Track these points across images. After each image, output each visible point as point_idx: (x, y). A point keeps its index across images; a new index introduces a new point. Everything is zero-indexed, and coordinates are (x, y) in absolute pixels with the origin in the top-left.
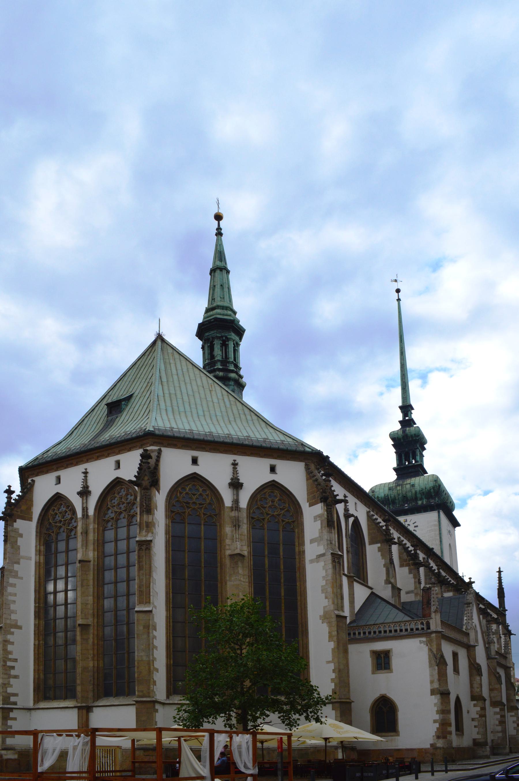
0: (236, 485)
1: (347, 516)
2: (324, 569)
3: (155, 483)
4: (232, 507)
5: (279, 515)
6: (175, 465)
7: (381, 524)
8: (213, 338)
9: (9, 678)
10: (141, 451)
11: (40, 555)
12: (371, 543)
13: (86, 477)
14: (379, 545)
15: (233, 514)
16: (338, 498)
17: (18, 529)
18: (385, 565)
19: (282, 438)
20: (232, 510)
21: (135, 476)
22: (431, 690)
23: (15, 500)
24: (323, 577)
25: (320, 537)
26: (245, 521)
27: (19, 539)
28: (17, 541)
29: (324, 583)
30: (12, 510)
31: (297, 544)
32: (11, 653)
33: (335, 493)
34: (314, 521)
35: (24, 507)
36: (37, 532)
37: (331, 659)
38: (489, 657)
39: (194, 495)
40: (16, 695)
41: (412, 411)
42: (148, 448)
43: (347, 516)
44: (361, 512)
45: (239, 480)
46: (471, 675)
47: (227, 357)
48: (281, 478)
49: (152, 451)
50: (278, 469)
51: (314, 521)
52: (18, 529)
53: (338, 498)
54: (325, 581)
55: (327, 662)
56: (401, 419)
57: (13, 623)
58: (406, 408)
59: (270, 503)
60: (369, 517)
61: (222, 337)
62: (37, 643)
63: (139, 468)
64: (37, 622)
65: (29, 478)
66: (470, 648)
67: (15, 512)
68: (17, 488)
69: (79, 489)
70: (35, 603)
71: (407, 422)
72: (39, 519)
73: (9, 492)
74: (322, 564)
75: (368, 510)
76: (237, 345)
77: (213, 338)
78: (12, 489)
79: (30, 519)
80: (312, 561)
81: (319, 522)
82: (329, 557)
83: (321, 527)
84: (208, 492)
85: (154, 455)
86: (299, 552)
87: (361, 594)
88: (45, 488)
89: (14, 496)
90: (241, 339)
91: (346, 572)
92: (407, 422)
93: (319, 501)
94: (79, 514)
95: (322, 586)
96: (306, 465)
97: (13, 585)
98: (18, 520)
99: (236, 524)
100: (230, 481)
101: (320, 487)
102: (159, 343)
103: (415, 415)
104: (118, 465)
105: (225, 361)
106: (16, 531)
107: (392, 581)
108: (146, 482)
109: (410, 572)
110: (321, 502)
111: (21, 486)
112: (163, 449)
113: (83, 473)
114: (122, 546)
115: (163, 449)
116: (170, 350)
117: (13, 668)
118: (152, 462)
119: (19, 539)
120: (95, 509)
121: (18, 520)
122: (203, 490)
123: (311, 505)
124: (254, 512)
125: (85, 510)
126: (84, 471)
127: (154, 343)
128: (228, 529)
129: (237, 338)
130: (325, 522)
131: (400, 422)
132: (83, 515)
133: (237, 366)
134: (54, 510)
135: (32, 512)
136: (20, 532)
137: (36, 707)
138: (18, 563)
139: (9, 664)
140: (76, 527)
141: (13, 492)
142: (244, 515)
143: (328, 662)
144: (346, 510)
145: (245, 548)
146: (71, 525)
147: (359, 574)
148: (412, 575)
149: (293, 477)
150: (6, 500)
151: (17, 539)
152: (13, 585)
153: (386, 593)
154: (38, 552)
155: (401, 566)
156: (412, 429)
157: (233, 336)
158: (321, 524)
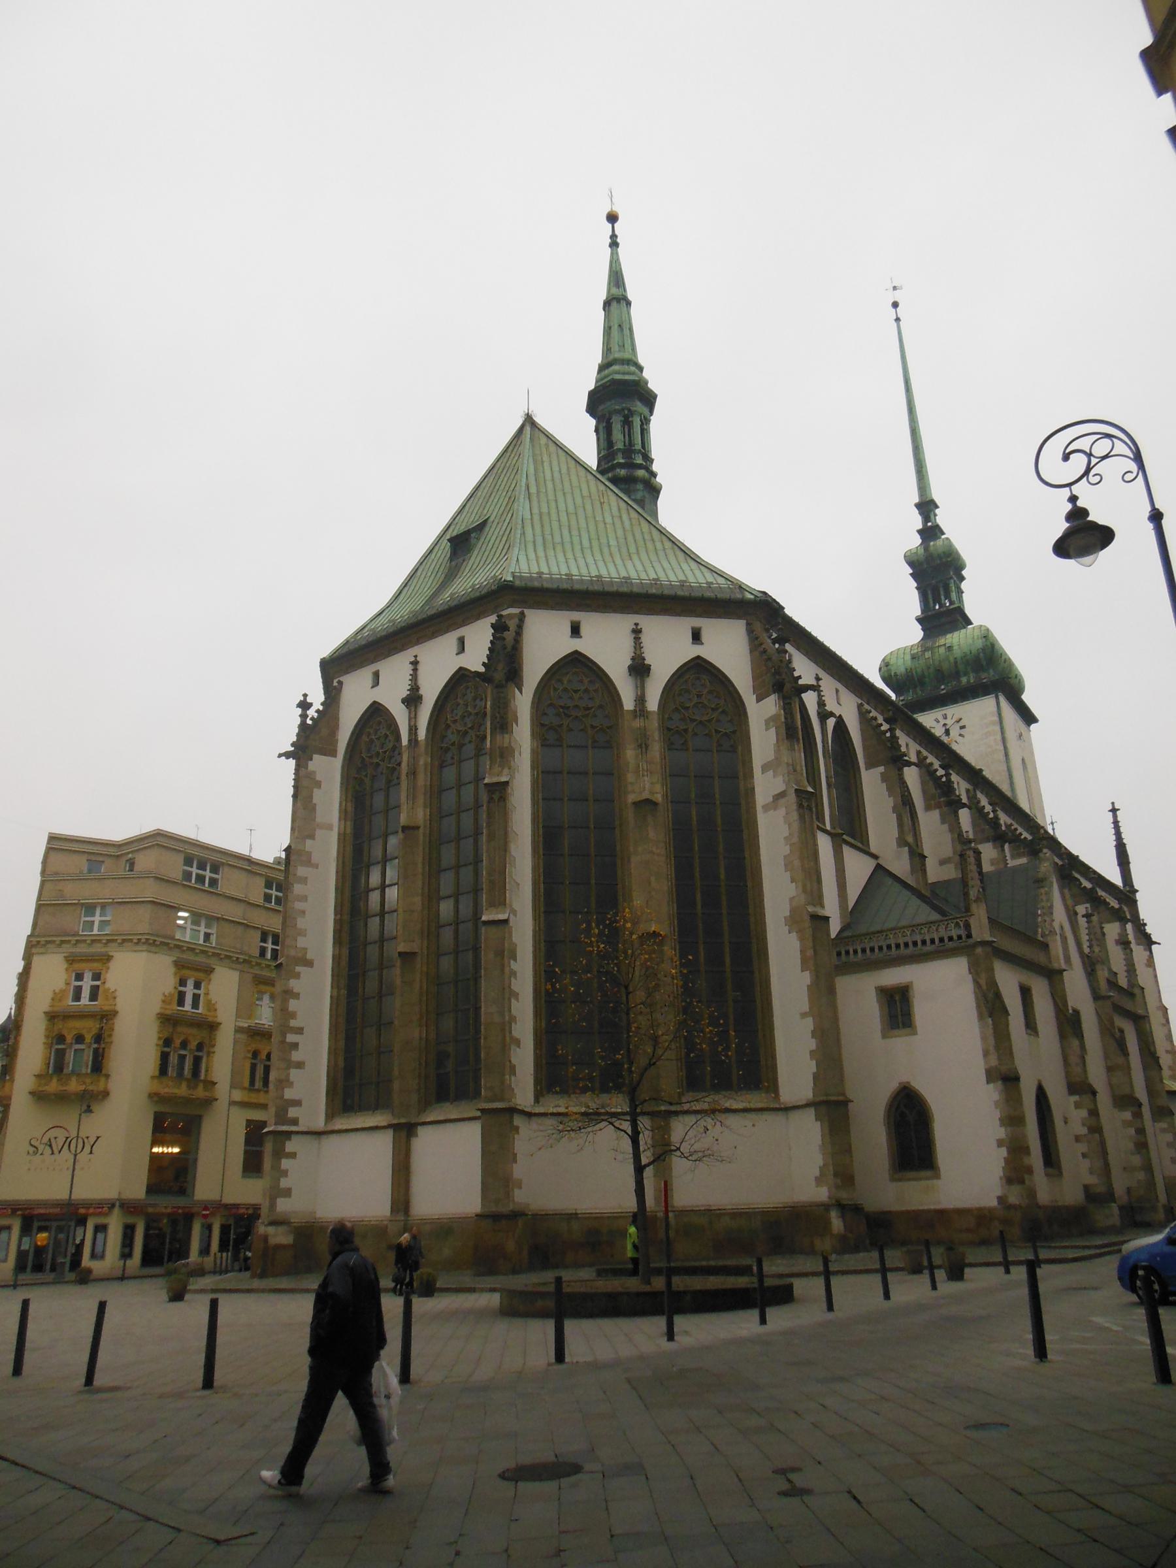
0: (639, 669)
1: (824, 715)
3: (514, 675)
4: (635, 711)
5: (709, 721)
6: (546, 640)
7: (883, 728)
8: (611, 413)
9: (288, 1068)
10: (493, 619)
11: (345, 820)
12: (870, 766)
13: (415, 670)
14: (882, 769)
15: (638, 723)
16: (801, 682)
17: (314, 772)
18: (895, 809)
19: (710, 578)
20: (636, 717)
21: (484, 664)
23: (312, 719)
25: (776, 758)
26: (656, 735)
27: (315, 790)
28: (311, 797)
31: (741, 775)
32: (293, 1015)
33: (796, 674)
38: (1097, 997)
39: (576, 691)
40: (297, 1103)
41: (937, 511)
42: (504, 613)
43: (824, 715)
44: (847, 707)
45: (644, 659)
46: (1062, 1036)
47: (631, 444)
49: (510, 616)
50: (705, 636)
53: (801, 682)
56: (920, 526)
57: (300, 955)
58: (927, 507)
59: (695, 700)
60: (863, 715)
61: (623, 409)
62: (335, 994)
63: (490, 649)
66: (1053, 976)
68: (317, 698)
71: (930, 532)
73: (304, 705)
75: (860, 701)
76: (645, 422)
77: (611, 413)
78: (309, 700)
79: (332, 753)
81: (773, 730)
84: (597, 685)
85: (512, 624)
87: (858, 869)
88: (357, 695)
89: (312, 713)
90: (651, 412)
91: (828, 827)
92: (930, 532)
96: (748, 624)
97: (304, 880)
98: (315, 756)
100: (629, 662)
101: (770, 664)
102: (528, 429)
103: (942, 518)
104: (461, 648)
105: (629, 451)
106: (311, 776)
107: (910, 839)
108: (499, 676)
109: (943, 821)
111: (325, 694)
112: (526, 611)
113: (411, 663)
114: (468, 793)
115: (526, 611)
116: (543, 440)
117: (295, 1046)
118: (509, 636)
119: (315, 790)
120: (428, 729)
121: (315, 756)
122: (590, 682)
123: (759, 699)
124: (670, 719)
125: (413, 730)
126: (413, 659)
127: (521, 430)
129: (645, 410)
131: (919, 532)
133: (648, 459)
134: (369, 734)
135: (337, 741)
136: (318, 778)
137: (330, 1128)
138: (312, 837)
139: (291, 1038)
141: (310, 705)
142: (654, 724)
144: (821, 704)
146: (393, 760)
147: (851, 830)
148: (946, 827)
150: (298, 721)
152: (304, 880)
153: (900, 865)
154: (344, 814)
155: (928, 808)
156: (939, 543)
157: (639, 407)
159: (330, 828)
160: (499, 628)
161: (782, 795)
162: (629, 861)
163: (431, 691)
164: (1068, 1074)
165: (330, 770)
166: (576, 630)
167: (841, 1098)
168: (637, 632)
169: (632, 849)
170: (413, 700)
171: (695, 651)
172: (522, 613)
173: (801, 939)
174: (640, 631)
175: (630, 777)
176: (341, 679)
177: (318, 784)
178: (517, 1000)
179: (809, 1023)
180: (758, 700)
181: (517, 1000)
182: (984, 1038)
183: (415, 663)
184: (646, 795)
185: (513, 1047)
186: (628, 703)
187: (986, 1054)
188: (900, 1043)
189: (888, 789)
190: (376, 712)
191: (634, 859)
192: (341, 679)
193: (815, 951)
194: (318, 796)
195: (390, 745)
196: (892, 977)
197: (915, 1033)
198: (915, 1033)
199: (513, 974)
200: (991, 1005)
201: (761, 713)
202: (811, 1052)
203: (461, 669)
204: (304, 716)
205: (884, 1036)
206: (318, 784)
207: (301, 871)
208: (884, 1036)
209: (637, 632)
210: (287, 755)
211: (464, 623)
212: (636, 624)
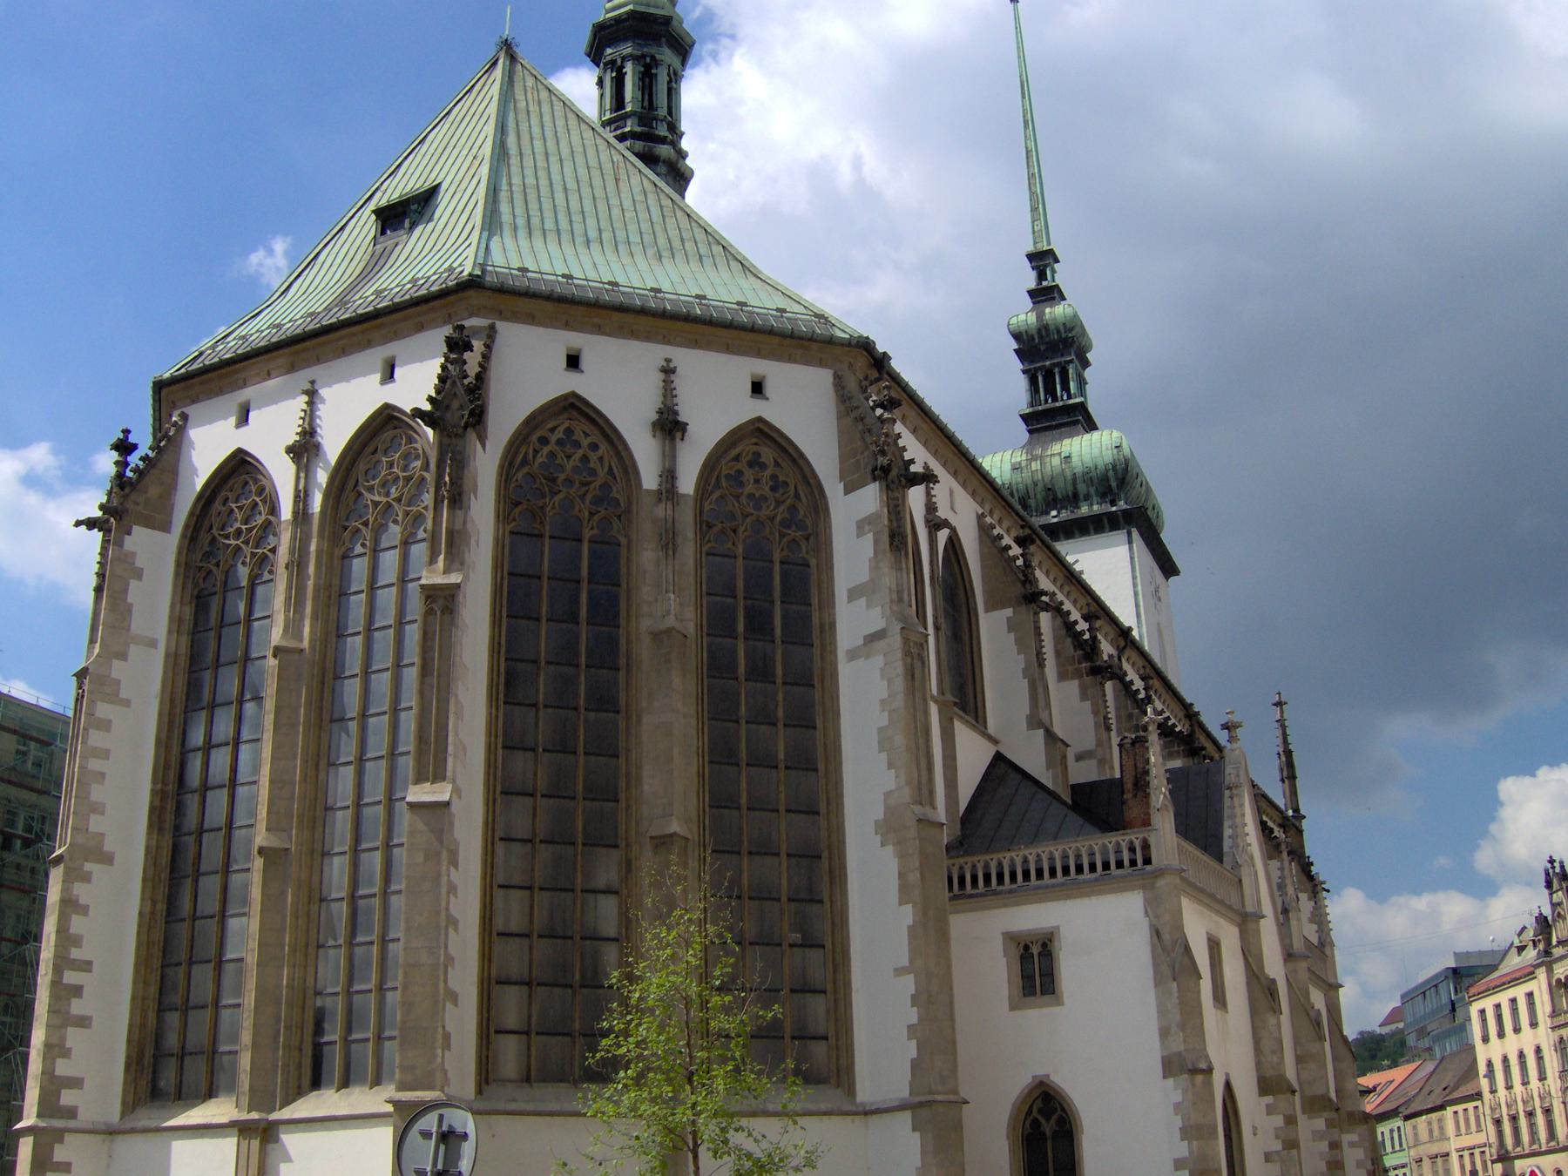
2: (882, 677)
15: (661, 511)
16: (913, 469)
17: (133, 554)
22: (1163, 1058)
23: (136, 470)
24: (882, 701)
25: (872, 580)
26: (690, 535)
27: (133, 583)
28: (126, 591)
29: (884, 720)
30: (126, 497)
31: (815, 601)
33: (907, 456)
34: (858, 536)
35: (154, 491)
36: (178, 564)
37: (905, 962)
48: (773, 411)
51: (858, 536)
52: (133, 554)
53: (913, 469)
54: (886, 714)
55: (896, 970)
64: (154, 843)
65: (174, 406)
67: (130, 505)
68: (144, 440)
69: (292, 438)
70: (154, 781)
72: (187, 526)
74: (878, 661)
78: (132, 439)
79: (165, 527)
80: (853, 655)
82: (895, 640)
83: (876, 552)
86: (822, 625)
89: (134, 459)
93: (870, 476)
94: (286, 512)
95: (880, 730)
97: (105, 725)
98: (136, 529)
99: (669, 542)
101: (869, 440)
106: (127, 559)
110: (874, 479)
119: (133, 583)
121: (136, 529)
125: (302, 498)
126: (307, 386)
128: (647, 556)
130: (885, 538)
132: (295, 513)
134: (226, 500)
135: (172, 507)
136: (138, 564)
138: (123, 656)
140: (273, 551)
141: (134, 447)
143: (900, 971)
145: (690, 612)
149: (804, 408)
151: (127, 585)
152: (105, 725)
154: (176, 621)
158: (876, 542)
159: (153, 644)
160: (457, 346)
161: (879, 635)
162: (639, 721)
163: (334, 441)
164: (1258, 1064)
165: (157, 552)
166: (573, 362)
167: (952, 1098)
168: (668, 371)
169: (644, 704)
170: (304, 449)
171: (751, 409)
172: (492, 327)
173: (902, 856)
174: (673, 371)
175: (646, 592)
176: (186, 410)
177: (138, 574)
178: (456, 930)
179: (908, 984)
180: (847, 491)
181: (456, 930)
182: (1162, 1012)
183: (312, 394)
184: (670, 622)
185: (448, 1005)
186: (650, 479)
187: (1164, 1033)
188: (1037, 1016)
189: (1018, 642)
190: (240, 466)
191: (647, 719)
192: (186, 410)
193: (922, 874)
194: (136, 592)
195: (260, 520)
196: (1031, 917)
197: (1059, 1002)
198: (1059, 1002)
199: (452, 888)
200: (1173, 961)
201: (852, 511)
202: (909, 1027)
203: (387, 406)
204: (122, 465)
205: (1013, 1007)
206: (138, 574)
207: (103, 710)
208: (1013, 1007)
209: (668, 371)
210: (91, 524)
211: (396, 336)
212: (668, 361)
